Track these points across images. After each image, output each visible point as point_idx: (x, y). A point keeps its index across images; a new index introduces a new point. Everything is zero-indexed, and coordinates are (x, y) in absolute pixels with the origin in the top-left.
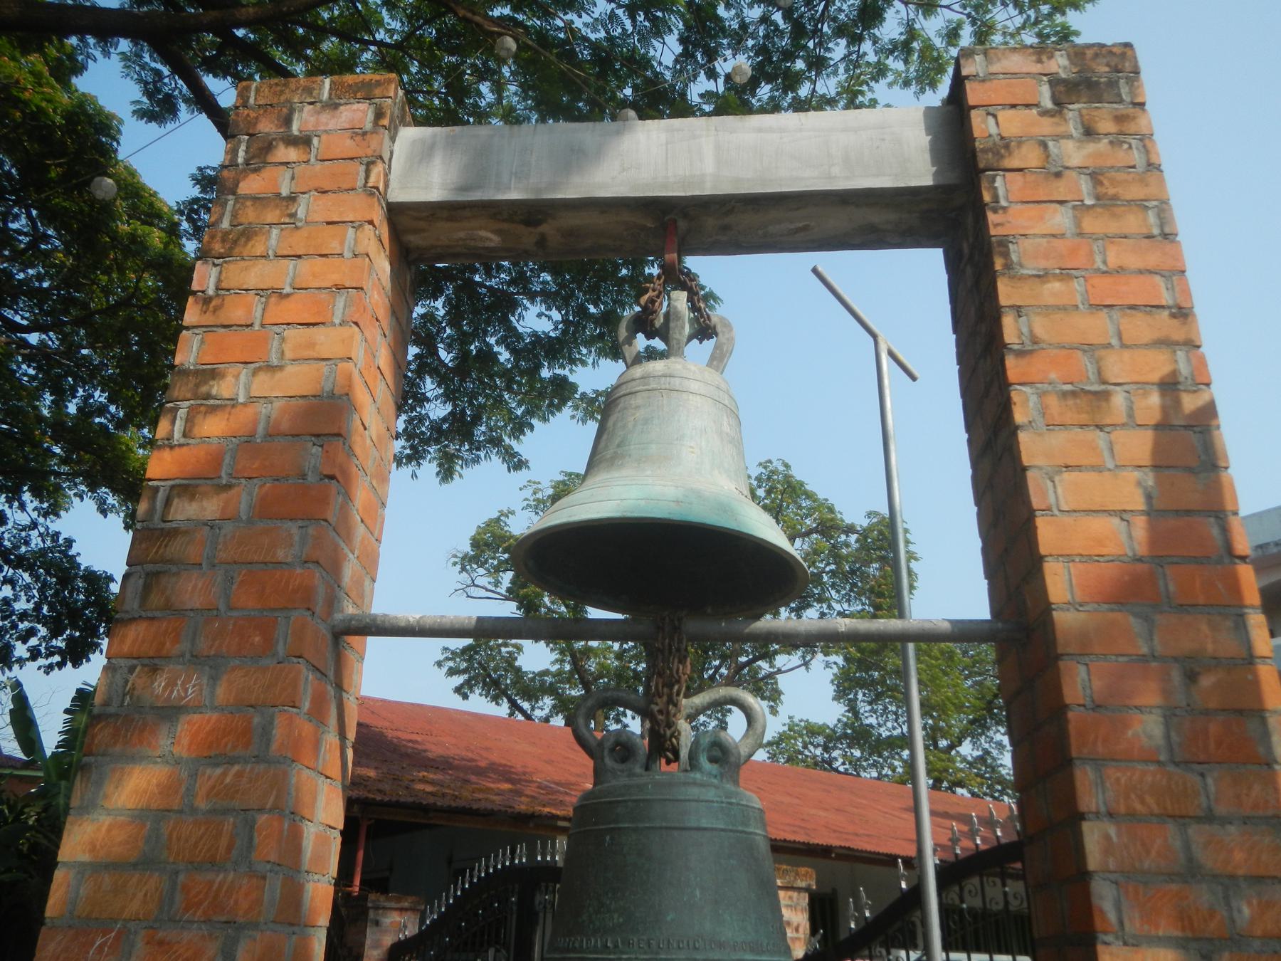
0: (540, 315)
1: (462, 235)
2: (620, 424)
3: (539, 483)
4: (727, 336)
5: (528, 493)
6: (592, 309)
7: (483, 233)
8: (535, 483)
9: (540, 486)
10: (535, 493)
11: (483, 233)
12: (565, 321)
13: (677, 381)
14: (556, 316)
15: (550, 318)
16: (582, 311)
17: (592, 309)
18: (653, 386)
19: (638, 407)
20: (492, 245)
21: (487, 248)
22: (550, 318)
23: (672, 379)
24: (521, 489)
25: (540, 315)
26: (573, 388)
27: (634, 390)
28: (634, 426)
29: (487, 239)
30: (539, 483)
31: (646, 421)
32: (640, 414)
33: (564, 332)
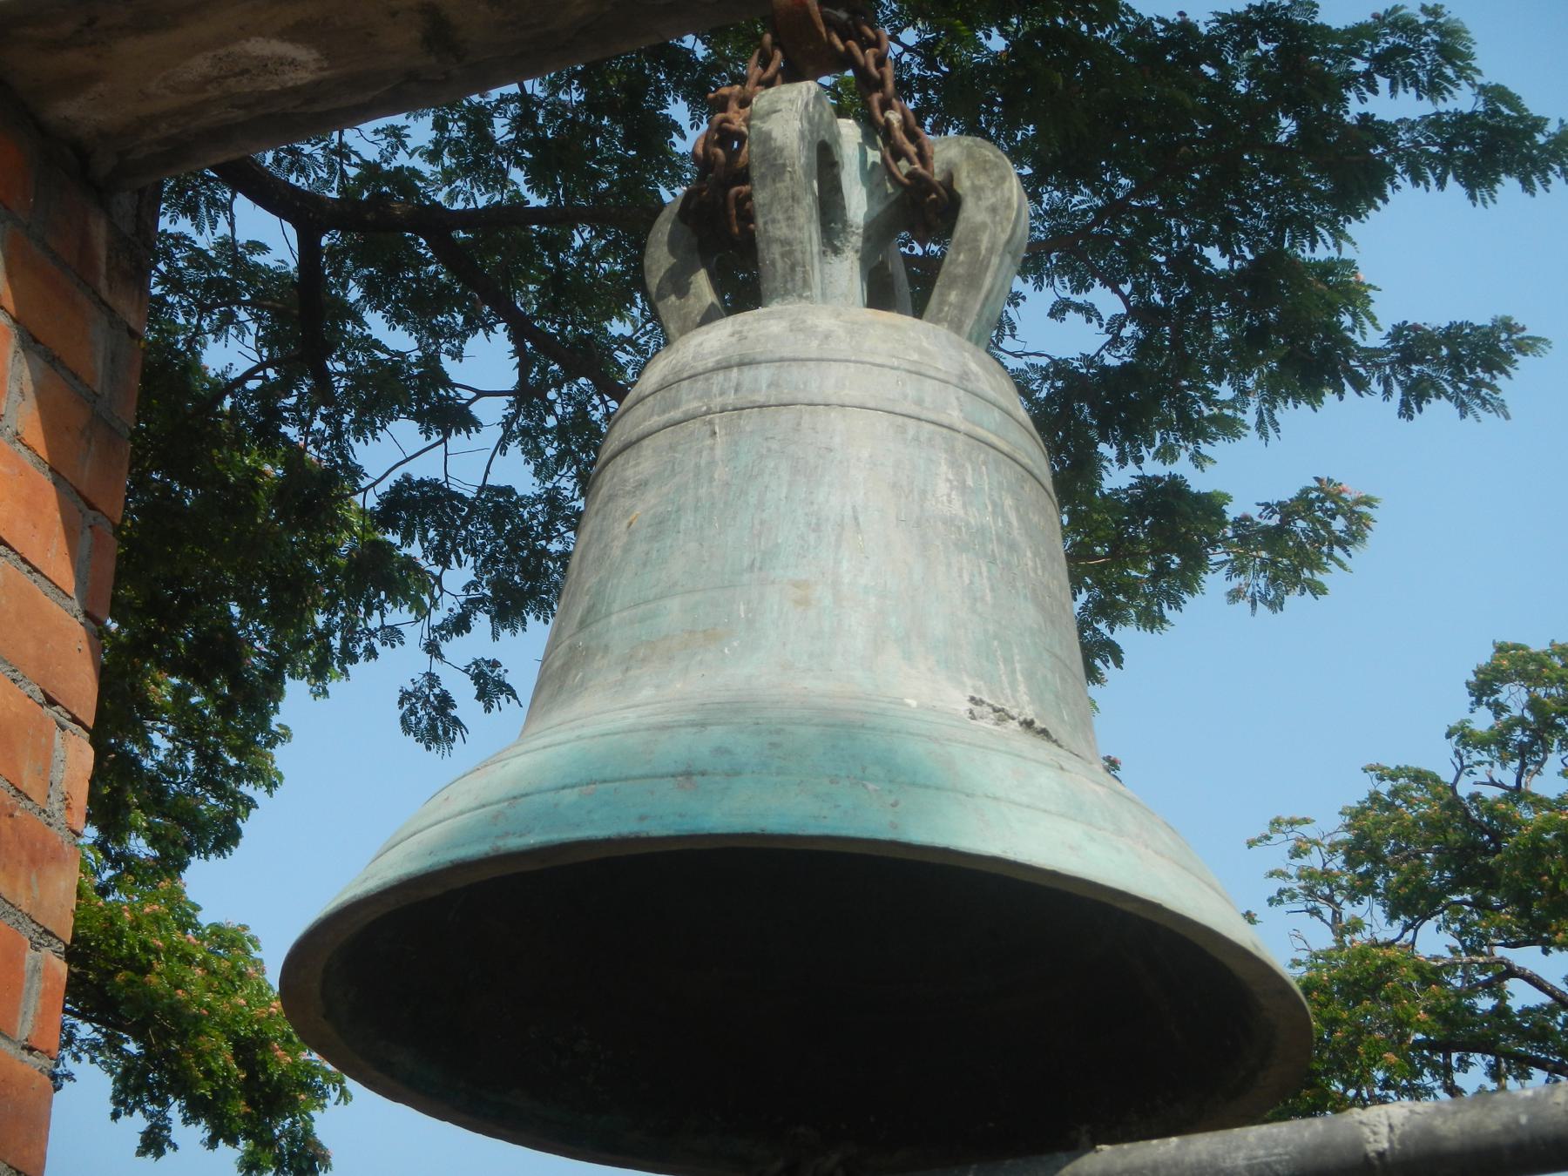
0: (1059, 310)
1: (200, 65)
2: (593, 553)
3: (1306, 821)
4: (990, 199)
5: (1277, 854)
6: (1217, 259)
7: (260, 47)
8: (1292, 823)
9: (1309, 831)
10: (1297, 853)
11: (260, 47)
12: (1140, 312)
13: (764, 374)
14: (1107, 301)
15: (1089, 311)
16: (1186, 265)
17: (1217, 259)
18: (691, 404)
19: (643, 485)
20: (303, 77)
21: (296, 90)
22: (1089, 311)
23: (748, 374)
24: (1251, 844)
25: (1059, 310)
26: (1211, 506)
27: (634, 435)
28: (627, 549)
29: (282, 60)
30: (1306, 821)
31: (660, 525)
32: (645, 506)
33: (1143, 347)
